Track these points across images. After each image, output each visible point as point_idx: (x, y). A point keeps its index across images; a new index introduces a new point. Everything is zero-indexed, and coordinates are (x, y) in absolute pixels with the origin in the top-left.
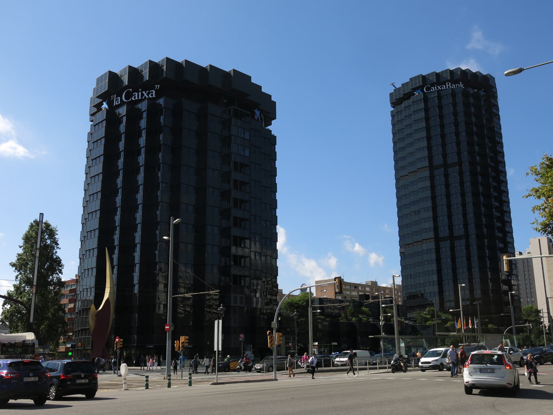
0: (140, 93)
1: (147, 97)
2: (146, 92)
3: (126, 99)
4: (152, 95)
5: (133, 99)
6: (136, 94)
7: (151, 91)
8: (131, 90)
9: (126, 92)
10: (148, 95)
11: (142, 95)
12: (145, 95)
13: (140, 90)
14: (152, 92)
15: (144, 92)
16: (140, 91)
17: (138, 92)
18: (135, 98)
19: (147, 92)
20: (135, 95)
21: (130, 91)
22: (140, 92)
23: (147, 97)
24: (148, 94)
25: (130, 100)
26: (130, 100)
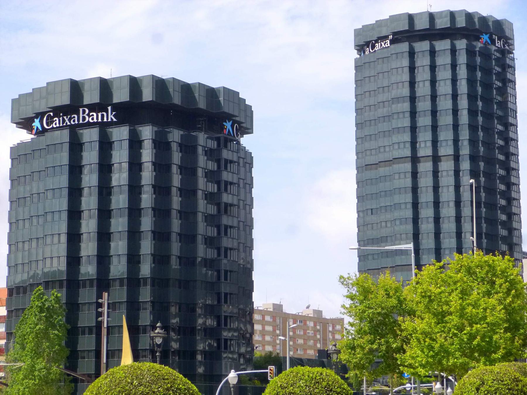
0: (61, 119)
2: (67, 118)
4: (74, 121)
5: (55, 126)
6: (56, 118)
7: (72, 116)
8: (52, 114)
9: (47, 116)
10: (70, 121)
11: (64, 121)
12: (67, 120)
13: (61, 114)
14: (74, 117)
15: (65, 117)
16: (60, 116)
17: (59, 117)
18: (56, 124)
19: (69, 117)
22: (62, 117)
23: (69, 124)
24: (70, 120)
26: (51, 126)
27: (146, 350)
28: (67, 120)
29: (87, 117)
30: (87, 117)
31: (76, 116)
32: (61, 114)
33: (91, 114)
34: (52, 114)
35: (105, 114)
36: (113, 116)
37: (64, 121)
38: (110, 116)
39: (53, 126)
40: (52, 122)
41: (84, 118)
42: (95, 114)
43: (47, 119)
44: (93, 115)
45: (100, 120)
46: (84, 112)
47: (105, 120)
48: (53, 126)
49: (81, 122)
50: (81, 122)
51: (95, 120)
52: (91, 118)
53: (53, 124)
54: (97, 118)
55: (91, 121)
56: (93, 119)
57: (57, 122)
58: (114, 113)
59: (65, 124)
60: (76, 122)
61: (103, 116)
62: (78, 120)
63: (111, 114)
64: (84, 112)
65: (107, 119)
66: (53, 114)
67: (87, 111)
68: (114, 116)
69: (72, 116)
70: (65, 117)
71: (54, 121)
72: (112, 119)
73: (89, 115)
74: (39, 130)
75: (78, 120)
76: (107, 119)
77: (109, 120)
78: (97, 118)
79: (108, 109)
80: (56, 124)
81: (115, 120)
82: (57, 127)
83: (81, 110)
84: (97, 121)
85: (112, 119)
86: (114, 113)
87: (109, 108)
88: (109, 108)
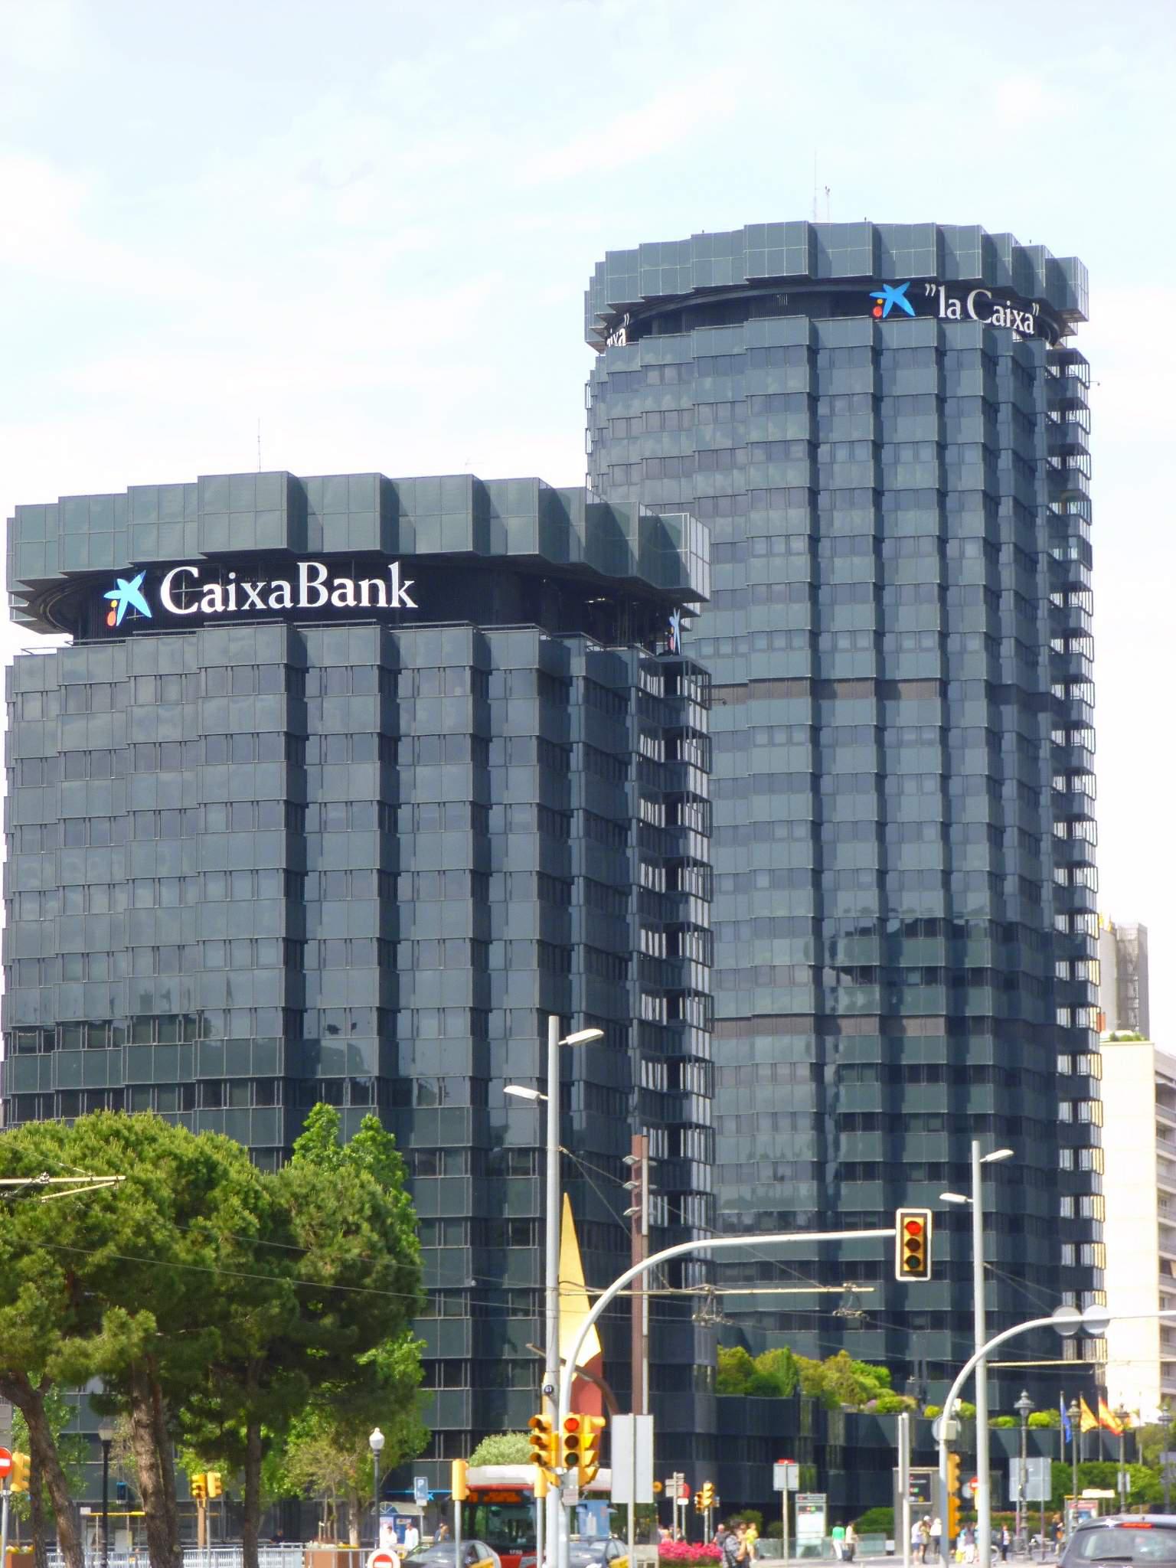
0: (232, 588)
1: (260, 605)
2: (254, 587)
3: (176, 599)
4: (280, 599)
5: (206, 609)
6: (217, 589)
7: (274, 584)
10: (265, 601)
11: (242, 596)
12: (253, 596)
15: (247, 586)
16: (230, 582)
19: (261, 585)
20: (211, 592)
21: (190, 574)
23: (260, 605)
24: (264, 595)
25: (194, 609)
26: (194, 609)
27: (456, 1292)
28: (253, 596)
29: (324, 592)
30: (324, 592)
31: (287, 586)
32: (232, 576)
33: (337, 582)
34: (195, 571)
35: (380, 584)
36: (407, 591)
37: (242, 596)
38: (398, 594)
39: (199, 607)
40: (198, 597)
41: (313, 594)
42: (349, 584)
43: (176, 583)
44: (343, 586)
45: (365, 602)
46: (313, 574)
47: (382, 602)
48: (199, 607)
49: (304, 602)
50: (304, 602)
51: (351, 602)
52: (336, 595)
53: (200, 602)
54: (358, 596)
55: (336, 602)
56: (343, 597)
57: (218, 596)
58: (408, 583)
59: (246, 607)
60: (288, 604)
61: (374, 590)
62: (295, 597)
63: (401, 585)
64: (313, 574)
65: (389, 600)
66: (200, 573)
67: (323, 572)
68: (408, 592)
69: (274, 584)
71: (202, 595)
72: (401, 601)
73: (328, 584)
74: (139, 612)
75: (295, 597)
76: (389, 600)
77: (395, 604)
78: (358, 596)
79: (389, 572)
80: (211, 603)
81: (410, 604)
82: (215, 616)
83: (303, 567)
84: (357, 606)
85: (401, 601)
86: (408, 583)
87: (395, 568)
88: (395, 568)
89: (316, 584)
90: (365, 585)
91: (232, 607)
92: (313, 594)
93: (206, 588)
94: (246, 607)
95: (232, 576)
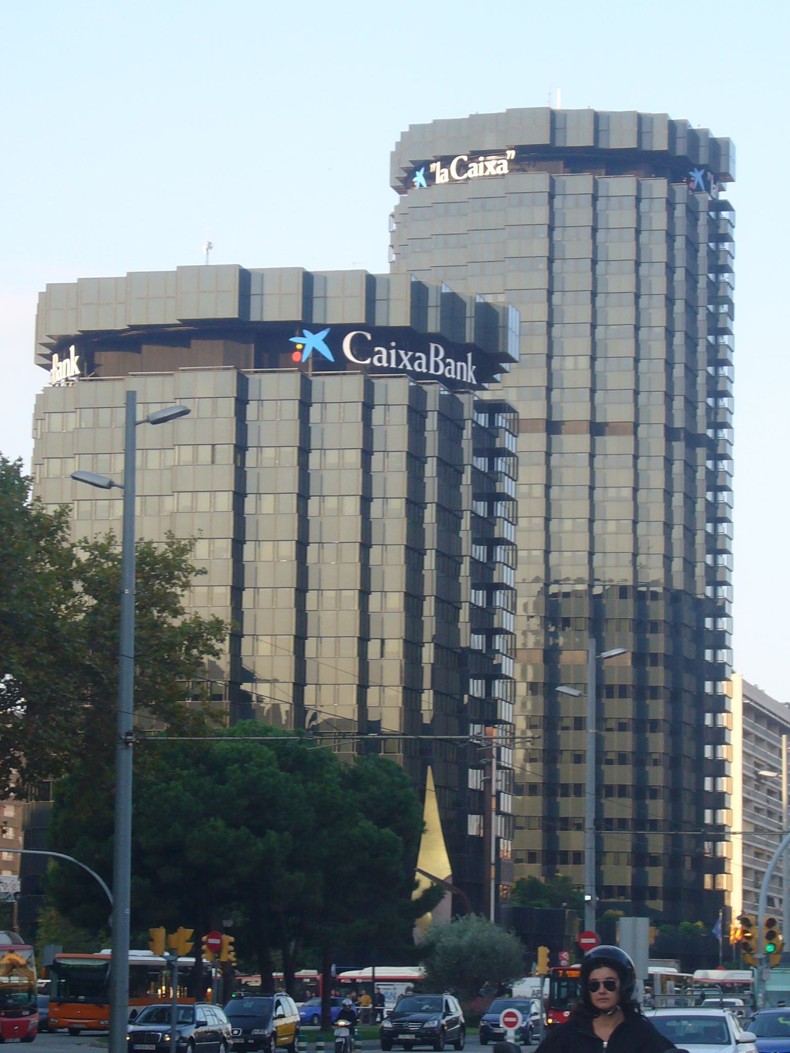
0: (393, 352)
1: (409, 368)
2: (406, 354)
10: (412, 366)
11: (399, 360)
15: (402, 353)
17: (389, 348)
19: (410, 353)
24: (412, 360)
30: (441, 365)
37: (399, 360)
41: (437, 368)
47: (465, 379)
48: (372, 361)
49: (432, 371)
59: (401, 367)
66: (372, 337)
70: (402, 353)
80: (380, 360)
83: (433, 346)
89: (437, 359)
90: (459, 364)
91: (393, 365)
92: (437, 368)
93: (377, 349)
94: (401, 367)
95: (393, 344)
